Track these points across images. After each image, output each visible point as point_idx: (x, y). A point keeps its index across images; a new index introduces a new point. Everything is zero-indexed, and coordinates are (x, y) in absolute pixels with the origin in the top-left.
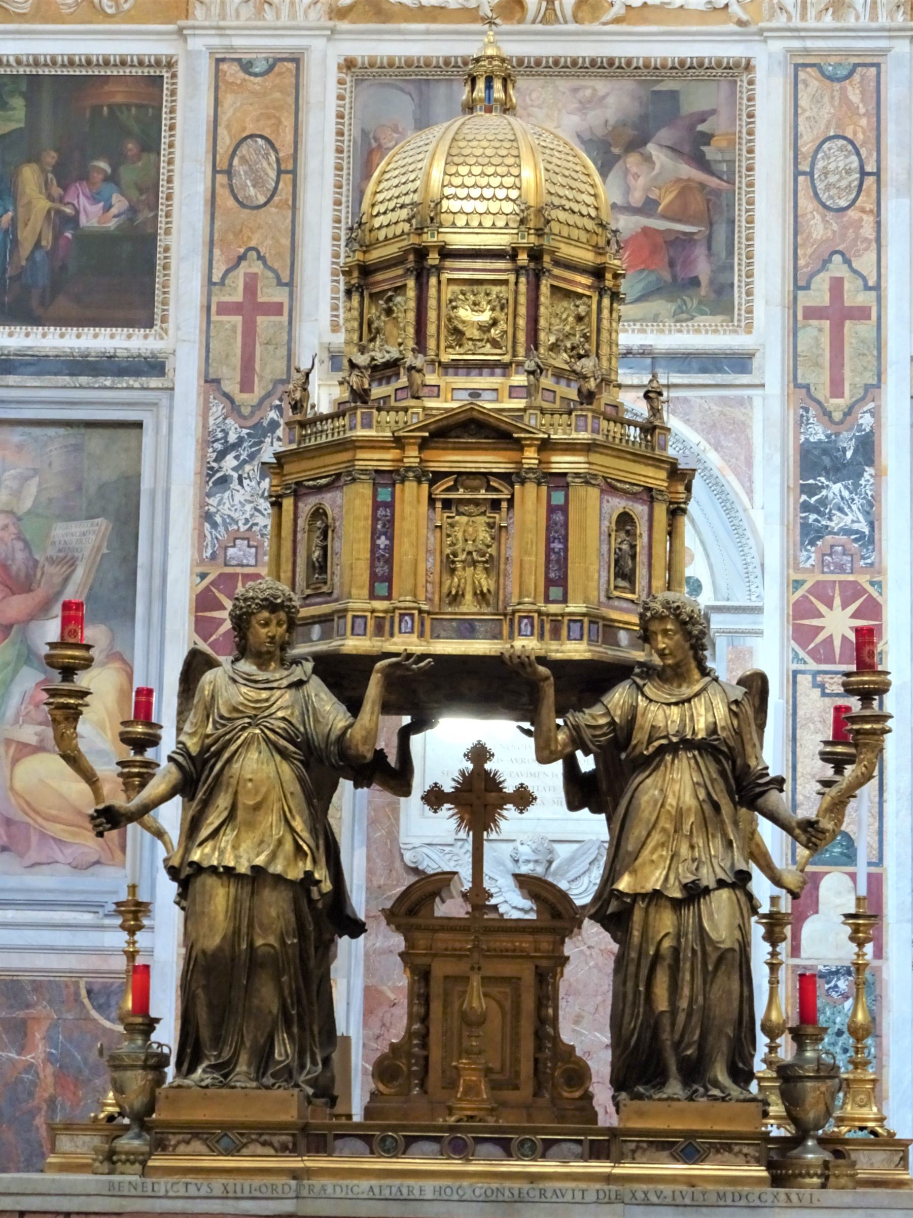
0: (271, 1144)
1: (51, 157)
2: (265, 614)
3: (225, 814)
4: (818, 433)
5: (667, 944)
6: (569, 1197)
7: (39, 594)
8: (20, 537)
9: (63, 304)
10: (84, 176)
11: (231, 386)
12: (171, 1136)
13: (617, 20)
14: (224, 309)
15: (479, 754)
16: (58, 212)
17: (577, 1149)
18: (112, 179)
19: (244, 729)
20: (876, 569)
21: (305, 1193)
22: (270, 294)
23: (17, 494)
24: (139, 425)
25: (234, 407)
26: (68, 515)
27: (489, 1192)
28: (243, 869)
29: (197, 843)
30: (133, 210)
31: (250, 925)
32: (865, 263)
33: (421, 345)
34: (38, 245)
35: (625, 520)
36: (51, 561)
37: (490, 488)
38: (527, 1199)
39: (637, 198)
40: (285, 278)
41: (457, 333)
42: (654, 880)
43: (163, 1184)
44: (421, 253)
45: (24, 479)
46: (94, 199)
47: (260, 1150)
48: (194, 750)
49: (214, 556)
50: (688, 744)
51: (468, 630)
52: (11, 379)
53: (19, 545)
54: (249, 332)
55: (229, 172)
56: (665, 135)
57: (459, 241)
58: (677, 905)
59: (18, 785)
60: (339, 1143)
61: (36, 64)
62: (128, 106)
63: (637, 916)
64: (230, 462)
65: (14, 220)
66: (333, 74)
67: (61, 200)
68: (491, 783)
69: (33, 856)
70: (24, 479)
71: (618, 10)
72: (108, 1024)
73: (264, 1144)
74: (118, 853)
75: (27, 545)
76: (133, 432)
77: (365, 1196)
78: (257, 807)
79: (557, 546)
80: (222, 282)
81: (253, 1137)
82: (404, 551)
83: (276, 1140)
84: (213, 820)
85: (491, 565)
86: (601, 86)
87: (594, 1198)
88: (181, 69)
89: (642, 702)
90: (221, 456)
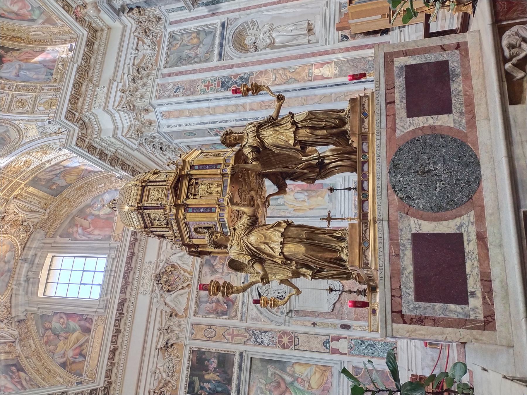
0: (366, 230)
1: (204, 372)
2: (214, 237)
3: (266, 246)
5: (308, 130)
6: (379, 143)
7: (281, 380)
8: (270, 384)
9: (229, 372)
10: (208, 366)
11: (246, 339)
12: (364, 262)
13: (193, 269)
14: (232, 340)
16: (213, 371)
17: (365, 144)
18: (209, 360)
19: (243, 241)
21: (381, 218)
22: (230, 331)
23: (262, 383)
24: (251, 358)
26: (267, 374)
27: (378, 165)
28: (282, 240)
29: (274, 254)
30: (214, 357)
31: (299, 238)
34: (218, 376)
36: (275, 377)
37: (192, 185)
38: (380, 154)
39: (221, 266)
40: (228, 328)
45: (260, 382)
46: (212, 364)
47: (368, 233)
48: (250, 258)
49: (275, 345)
50: (258, 131)
52: (241, 383)
53: (271, 384)
54: (237, 335)
55: (210, 338)
56: (212, 262)
58: (298, 128)
59: (316, 388)
60: (365, 210)
61: (188, 374)
62: (197, 357)
63: (300, 139)
64: (258, 340)
65: (214, 380)
66: (196, 318)
67: (211, 371)
69: (330, 386)
70: (260, 382)
71: (192, 269)
72: (362, 372)
73: (366, 232)
74: (329, 368)
75: (271, 382)
77: (381, 200)
78: (265, 237)
79: (208, 167)
80: (228, 340)
81: (363, 236)
83: (364, 229)
84: (269, 250)
86: (203, 272)
87: (379, 137)
88: (192, 346)
89: (248, 144)
90: (258, 342)
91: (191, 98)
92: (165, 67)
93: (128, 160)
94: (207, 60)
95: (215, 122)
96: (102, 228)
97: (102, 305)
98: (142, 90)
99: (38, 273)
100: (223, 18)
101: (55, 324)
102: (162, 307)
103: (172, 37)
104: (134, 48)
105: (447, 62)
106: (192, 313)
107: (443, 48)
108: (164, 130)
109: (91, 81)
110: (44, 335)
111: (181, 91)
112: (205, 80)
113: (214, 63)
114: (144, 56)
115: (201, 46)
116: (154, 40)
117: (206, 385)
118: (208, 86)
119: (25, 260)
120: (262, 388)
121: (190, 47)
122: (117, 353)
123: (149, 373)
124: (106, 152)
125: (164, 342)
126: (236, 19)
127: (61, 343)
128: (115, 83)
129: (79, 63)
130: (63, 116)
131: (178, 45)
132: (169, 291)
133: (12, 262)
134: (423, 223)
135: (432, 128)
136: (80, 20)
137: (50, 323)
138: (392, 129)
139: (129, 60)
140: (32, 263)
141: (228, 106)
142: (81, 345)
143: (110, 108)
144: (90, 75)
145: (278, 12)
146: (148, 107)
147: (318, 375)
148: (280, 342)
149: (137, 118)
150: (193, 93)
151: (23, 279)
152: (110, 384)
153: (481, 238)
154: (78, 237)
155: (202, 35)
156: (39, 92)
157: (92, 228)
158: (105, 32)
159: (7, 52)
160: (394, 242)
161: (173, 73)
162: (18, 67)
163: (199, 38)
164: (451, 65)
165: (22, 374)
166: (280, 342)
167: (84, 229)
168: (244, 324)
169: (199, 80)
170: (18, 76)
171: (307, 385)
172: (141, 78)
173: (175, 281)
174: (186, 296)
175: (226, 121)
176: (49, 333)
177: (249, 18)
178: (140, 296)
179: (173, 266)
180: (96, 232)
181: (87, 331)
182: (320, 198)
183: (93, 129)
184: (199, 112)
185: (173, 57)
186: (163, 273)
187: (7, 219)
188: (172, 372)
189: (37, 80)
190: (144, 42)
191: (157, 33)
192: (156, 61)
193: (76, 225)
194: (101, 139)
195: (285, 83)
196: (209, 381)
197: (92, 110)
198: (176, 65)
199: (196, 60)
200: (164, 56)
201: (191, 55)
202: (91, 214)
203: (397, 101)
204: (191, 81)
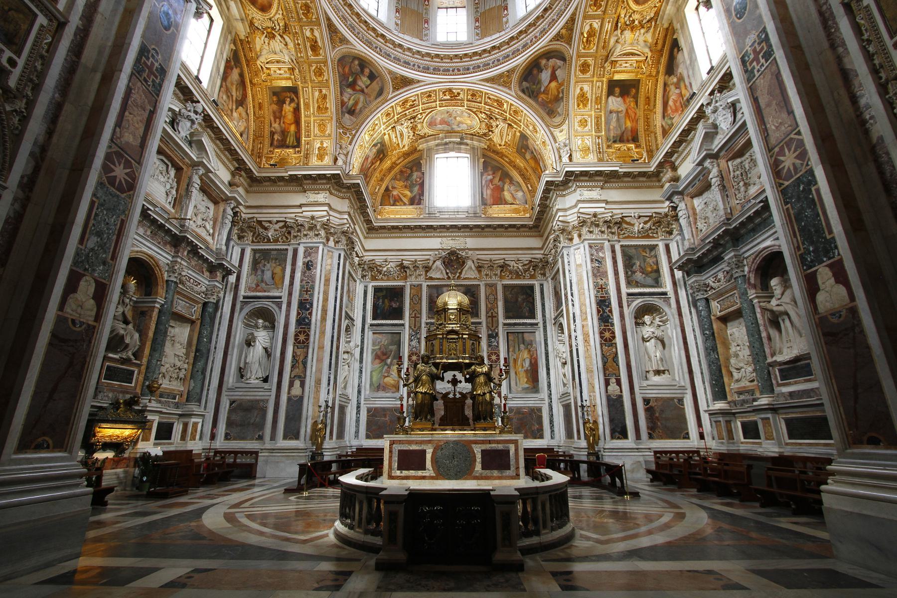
4: (490, 332)
10: (393, 300)
15: (454, 376)
18: (397, 301)
20: (499, 350)
25: (413, 330)
32: (496, 310)
33: (445, 321)
35: (473, 343)
41: (450, 320)
42: (479, 392)
43: (413, 436)
44: (445, 309)
51: (453, 359)
57: (450, 307)
68: (456, 379)
76: (398, 335)
82: (444, 348)
85: (456, 350)
91: (590, 274)
92: (622, 246)
93: (547, 215)
94: (629, 283)
95: (572, 295)
96: (492, 196)
97: (432, 210)
98: (596, 230)
99: (452, 150)
100: (671, 294)
101: (415, 175)
102: (432, 259)
103: (653, 248)
104: (641, 214)
105: (509, 469)
106: (429, 284)
107: (517, 468)
108: (565, 253)
109: (606, 182)
110: (407, 168)
111: (597, 265)
112: (607, 285)
113: (624, 290)
114: (633, 225)
115: (644, 276)
116: (650, 232)
117: (381, 300)
118: (601, 288)
119: (462, 138)
120: (381, 342)
121: (642, 265)
122: (397, 231)
123: (385, 257)
124: (549, 201)
125: (407, 265)
126: (670, 305)
127: (401, 183)
128: (604, 205)
129: (620, 170)
130: (567, 169)
131: (645, 254)
132: (444, 263)
133: (459, 129)
134: (431, 455)
135: (475, 460)
136: (661, 165)
137: (416, 171)
138: (476, 442)
139: (626, 213)
140: (460, 143)
141: (585, 305)
142: (402, 200)
143: (580, 205)
144: (612, 180)
145: (675, 343)
146: (583, 238)
147: (392, 382)
148: (412, 354)
149: (574, 227)
150: (594, 275)
151: (447, 140)
152: (377, 230)
153: (424, 478)
154: (484, 177)
155: (654, 275)
156: (596, 136)
157: (492, 187)
158: (657, 184)
159: (633, 97)
160: (422, 442)
161: (615, 255)
162: (620, 110)
163: (651, 272)
164: (508, 471)
165: (379, 162)
166: (412, 354)
167: (491, 181)
168: (423, 325)
169: (608, 279)
170: (611, 112)
171: (386, 375)
172: (609, 227)
173: (453, 266)
174: (441, 277)
175: (573, 305)
176: (409, 171)
177: (670, 317)
178: (439, 240)
179: (464, 263)
180: (489, 192)
181: (412, 202)
182: (526, 380)
183: (564, 190)
184: (580, 281)
185: (632, 252)
186: (457, 256)
187: (491, 121)
188: (388, 276)
189: (608, 130)
190: (645, 223)
191: (657, 233)
192: (628, 237)
193: (494, 174)
194: (556, 198)
195: (603, 354)
196: (383, 302)
197: (578, 189)
198: (624, 254)
199: (630, 273)
200: (633, 243)
201: (634, 268)
202: (504, 183)
203: (490, 445)
204: (606, 272)
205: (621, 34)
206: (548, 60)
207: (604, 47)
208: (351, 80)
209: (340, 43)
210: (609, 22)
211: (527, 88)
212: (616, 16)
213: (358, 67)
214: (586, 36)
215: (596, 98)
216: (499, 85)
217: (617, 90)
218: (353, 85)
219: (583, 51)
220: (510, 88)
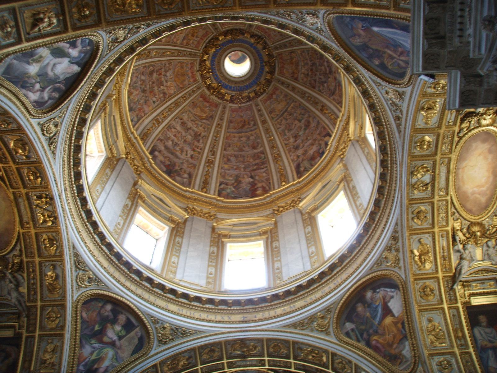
205: (464, 248)
206: (374, 291)
207: (444, 267)
208: (97, 328)
209: (89, 282)
210: (442, 237)
211: (353, 330)
212: (449, 228)
213: (110, 314)
214: (417, 254)
215: (455, 331)
216: (312, 331)
217: (483, 319)
218: (99, 335)
219: (418, 272)
220: (328, 334)
